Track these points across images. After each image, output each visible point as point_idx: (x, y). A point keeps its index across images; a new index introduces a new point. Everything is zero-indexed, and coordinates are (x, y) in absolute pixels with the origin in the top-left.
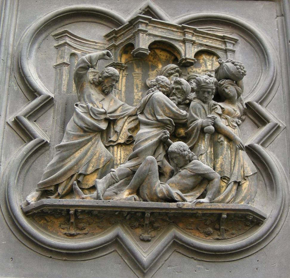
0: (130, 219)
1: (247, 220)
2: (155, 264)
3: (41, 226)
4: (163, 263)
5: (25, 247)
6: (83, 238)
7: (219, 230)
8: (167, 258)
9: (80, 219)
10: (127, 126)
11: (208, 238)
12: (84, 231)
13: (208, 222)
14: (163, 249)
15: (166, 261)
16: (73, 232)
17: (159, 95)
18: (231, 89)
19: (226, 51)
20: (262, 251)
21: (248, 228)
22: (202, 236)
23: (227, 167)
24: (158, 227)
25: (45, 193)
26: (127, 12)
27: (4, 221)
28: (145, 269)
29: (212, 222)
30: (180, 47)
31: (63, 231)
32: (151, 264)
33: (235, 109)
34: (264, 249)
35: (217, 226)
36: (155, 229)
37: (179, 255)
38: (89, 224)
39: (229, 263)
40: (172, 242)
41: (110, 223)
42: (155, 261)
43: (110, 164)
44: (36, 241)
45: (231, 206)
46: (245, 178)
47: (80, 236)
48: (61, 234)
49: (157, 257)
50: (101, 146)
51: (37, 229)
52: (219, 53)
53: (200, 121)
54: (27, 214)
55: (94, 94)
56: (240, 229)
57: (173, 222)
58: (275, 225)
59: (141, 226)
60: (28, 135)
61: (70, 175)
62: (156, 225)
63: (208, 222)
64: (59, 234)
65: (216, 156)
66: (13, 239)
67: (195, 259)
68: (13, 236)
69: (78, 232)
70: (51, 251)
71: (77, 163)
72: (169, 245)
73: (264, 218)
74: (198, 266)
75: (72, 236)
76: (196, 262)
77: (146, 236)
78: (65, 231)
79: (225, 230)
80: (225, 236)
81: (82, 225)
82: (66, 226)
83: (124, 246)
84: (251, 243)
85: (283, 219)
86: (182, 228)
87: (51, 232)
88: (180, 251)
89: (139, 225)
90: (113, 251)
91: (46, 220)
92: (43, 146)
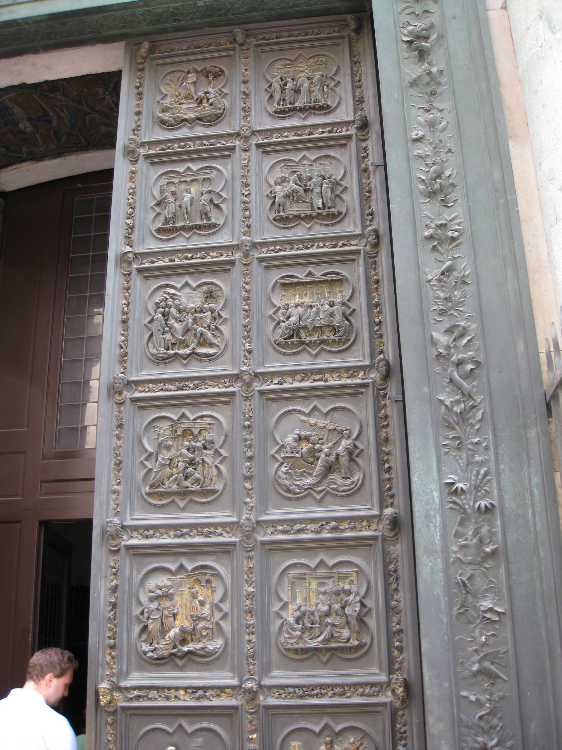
10: (177, 461)
17: (185, 451)
18: (208, 446)
19: (210, 428)
23: (207, 474)
25: (151, 487)
26: (176, 414)
30: (193, 430)
33: (212, 452)
43: (171, 475)
45: (209, 488)
46: (214, 476)
50: (168, 469)
52: (208, 429)
53: (198, 459)
54: (147, 494)
55: (164, 451)
59: (181, 495)
60: (146, 467)
61: (159, 480)
65: (204, 470)
71: (160, 476)
92: (150, 470)
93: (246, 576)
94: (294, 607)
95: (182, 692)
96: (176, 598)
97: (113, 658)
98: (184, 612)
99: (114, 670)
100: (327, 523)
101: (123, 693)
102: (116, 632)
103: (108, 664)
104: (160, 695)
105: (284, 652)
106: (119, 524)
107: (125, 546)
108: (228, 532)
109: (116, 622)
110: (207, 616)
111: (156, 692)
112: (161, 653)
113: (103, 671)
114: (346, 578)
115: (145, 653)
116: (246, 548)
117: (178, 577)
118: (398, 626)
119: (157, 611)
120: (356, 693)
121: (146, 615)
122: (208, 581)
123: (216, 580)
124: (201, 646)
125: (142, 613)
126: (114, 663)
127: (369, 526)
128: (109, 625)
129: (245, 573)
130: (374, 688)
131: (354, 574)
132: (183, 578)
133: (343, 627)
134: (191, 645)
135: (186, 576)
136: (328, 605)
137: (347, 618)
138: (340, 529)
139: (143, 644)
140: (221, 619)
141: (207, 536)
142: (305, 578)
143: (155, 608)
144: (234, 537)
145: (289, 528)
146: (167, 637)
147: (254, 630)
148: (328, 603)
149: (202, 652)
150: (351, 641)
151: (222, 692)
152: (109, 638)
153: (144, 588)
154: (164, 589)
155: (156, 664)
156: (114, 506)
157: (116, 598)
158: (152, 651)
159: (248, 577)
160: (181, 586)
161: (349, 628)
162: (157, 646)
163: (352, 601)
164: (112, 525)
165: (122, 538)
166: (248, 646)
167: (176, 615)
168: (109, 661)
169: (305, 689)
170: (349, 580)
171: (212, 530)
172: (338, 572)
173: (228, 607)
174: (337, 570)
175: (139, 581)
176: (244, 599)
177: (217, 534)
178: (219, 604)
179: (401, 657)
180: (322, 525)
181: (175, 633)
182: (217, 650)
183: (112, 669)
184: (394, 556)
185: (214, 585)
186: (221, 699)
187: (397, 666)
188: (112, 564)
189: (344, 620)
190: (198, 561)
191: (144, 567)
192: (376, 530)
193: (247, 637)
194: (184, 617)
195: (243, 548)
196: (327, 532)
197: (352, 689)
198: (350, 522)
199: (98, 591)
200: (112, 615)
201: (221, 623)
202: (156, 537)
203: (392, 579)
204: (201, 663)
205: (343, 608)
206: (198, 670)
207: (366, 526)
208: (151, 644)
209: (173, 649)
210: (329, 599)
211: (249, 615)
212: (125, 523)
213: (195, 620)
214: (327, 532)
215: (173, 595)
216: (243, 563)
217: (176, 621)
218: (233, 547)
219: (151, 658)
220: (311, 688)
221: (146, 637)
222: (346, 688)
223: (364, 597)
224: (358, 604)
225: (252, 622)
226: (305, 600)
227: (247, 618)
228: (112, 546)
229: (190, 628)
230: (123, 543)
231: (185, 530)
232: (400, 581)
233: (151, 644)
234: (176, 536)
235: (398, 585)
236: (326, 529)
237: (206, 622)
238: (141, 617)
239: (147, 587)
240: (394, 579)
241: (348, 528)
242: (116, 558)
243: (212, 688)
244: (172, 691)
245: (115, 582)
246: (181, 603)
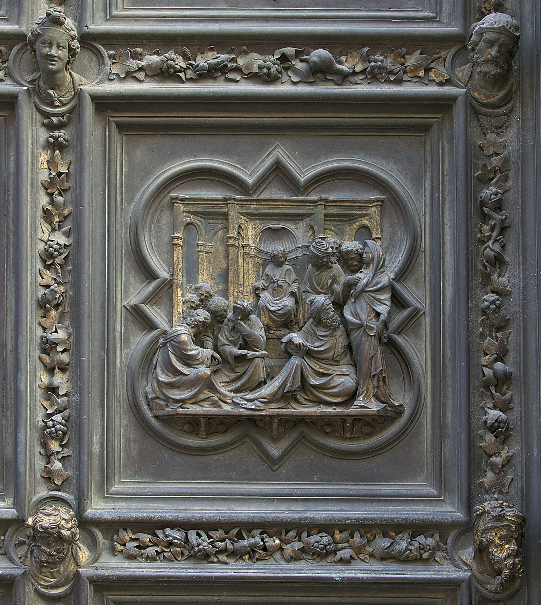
93: (44, 200)
94: (189, 296)
100: (297, 54)
105: (154, 423)
114: (350, 218)
116: (47, 115)
118: (499, 365)
120: (369, 549)
127: (427, 70)
130: (421, 539)
131: (373, 210)
133: (335, 362)
136: (293, 294)
137: (348, 334)
138: (340, 73)
142: (226, 216)
144: (8, 81)
145: (181, 63)
147: (65, 357)
148: (294, 288)
150: (360, 401)
159: (52, 202)
161: (355, 365)
163: (367, 285)
166: (46, 404)
169: (216, 535)
170: (356, 226)
172: (326, 200)
174: (323, 196)
179: (504, 454)
180: (284, 58)
184: (495, 161)
187: (489, 477)
189: (340, 340)
192: (448, 82)
193: (44, 378)
195: (39, 116)
196: (295, 79)
197: (357, 538)
198: (368, 54)
203: (487, 228)
205: (339, 306)
207: (416, 68)
210: (294, 276)
211: (54, 313)
214: (295, 79)
216: (35, 162)
220: (235, 531)
222: (338, 536)
223: (401, 276)
224: (386, 296)
225: (61, 335)
226: (225, 277)
227: (47, 323)
232: (511, 235)
235: (503, 247)
236: (296, 72)
240: (492, 229)
241: (363, 72)
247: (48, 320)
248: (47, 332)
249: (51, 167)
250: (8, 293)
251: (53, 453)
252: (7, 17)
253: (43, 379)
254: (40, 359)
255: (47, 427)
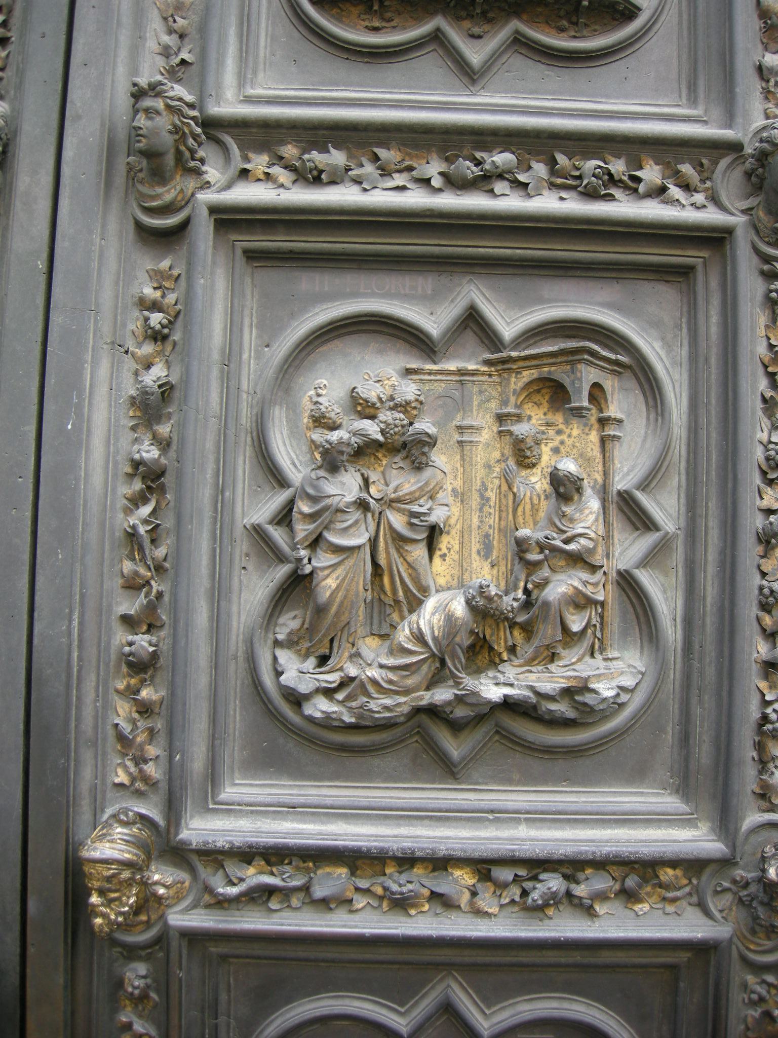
0: (455, 6)
1: (616, 11)
2: (489, 68)
3: (332, 16)
4: (498, 67)
5: (312, 45)
6: (391, 32)
7: (576, 24)
8: (504, 61)
9: (386, 6)
11: (561, 35)
12: (393, 24)
13: (562, 13)
14: (500, 48)
15: (503, 64)
16: (377, 24)
20: (634, 55)
21: (616, 23)
22: (553, 32)
24: (493, 19)
27: (282, 10)
28: (475, 75)
29: (567, 13)
31: (362, 23)
32: (482, 67)
34: (637, 52)
35: (574, 19)
36: (490, 21)
37: (522, 57)
38: (399, 14)
39: (589, 70)
40: (512, 38)
41: (428, 13)
42: (489, 63)
44: (327, 36)
47: (387, 30)
48: (361, 28)
49: (491, 58)
51: (328, 20)
56: (605, 24)
57: (514, 12)
58: (653, 20)
59: (470, 16)
62: (491, 15)
63: (562, 13)
64: (358, 27)
66: (296, 34)
67: (543, 63)
68: (295, 30)
69: (384, 24)
70: (348, 50)
72: (508, 42)
73: (640, 9)
74: (547, 73)
75: (376, 29)
76: (543, 66)
77: (476, 30)
78: (367, 23)
79: (585, 25)
80: (585, 33)
81: (389, 15)
82: (367, 16)
83: (446, 43)
84: (620, 43)
85: (665, 12)
86: (527, 21)
87: (347, 25)
88: (523, 52)
89: (468, 15)
90: (432, 51)
91: (340, 8)
95: (465, 877)
96: (439, 458)
97: (145, 709)
98: (475, 521)
99: (150, 769)
101: (193, 871)
102: (160, 595)
103: (121, 738)
104: (363, 884)
106: (191, 106)
107: (214, 210)
108: (687, 187)
109: (160, 552)
110: (591, 551)
111: (343, 871)
112: (373, 705)
113: (101, 771)
115: (296, 699)
117: (452, 366)
119: (357, 515)
121: (302, 529)
122: (597, 393)
123: (621, 389)
124: (564, 684)
125: (285, 517)
126: (152, 733)
128: (128, 566)
129: (760, 371)
132: (474, 373)
134: (510, 671)
135: (488, 363)
139: (285, 657)
140: (646, 561)
141: (591, 194)
143: (350, 498)
146: (403, 635)
149: (561, 708)
151: (645, 880)
152: (128, 621)
153: (293, 409)
154: (386, 416)
155: (344, 748)
156: (166, 39)
157: (164, 445)
158: (329, 693)
160: (463, 405)
162: (353, 671)
164: (160, 104)
165: (198, 173)
166: (763, 685)
167: (441, 532)
168: (126, 728)
171: (618, 167)
173: (673, 511)
175: (270, 372)
176: (758, 480)
177: (642, 188)
178: (640, 495)
181: (450, 618)
182: (624, 698)
183: (140, 760)
185: (613, 411)
186: (637, 907)
188: (149, 292)
190: (541, 301)
191: (293, 316)
194: (475, 547)
195: (755, 260)
199: (79, 406)
200: (145, 522)
201: (645, 578)
202: (357, 181)
204: (549, 751)
206: (530, 779)
208: (323, 660)
209: (430, 686)
212: (216, 110)
213: (532, 567)
215: (427, 442)
217: (437, 560)
218: (705, 254)
219: (327, 723)
221: (295, 624)
228: (150, 211)
229: (510, 603)
230: (205, 197)
231: (502, 158)
233: (323, 660)
234: (455, 183)
237: (585, 575)
238: (278, 535)
239: (306, 405)
242: (165, 264)
243: (601, 864)
244: (418, 871)
245: (158, 371)
246: (458, 484)
247: (770, 562)
248: (769, 579)
249: (771, 335)
250: (709, 518)
251: (773, 758)
252: (705, 119)
253: (760, 649)
254: (758, 619)
255: (765, 719)
